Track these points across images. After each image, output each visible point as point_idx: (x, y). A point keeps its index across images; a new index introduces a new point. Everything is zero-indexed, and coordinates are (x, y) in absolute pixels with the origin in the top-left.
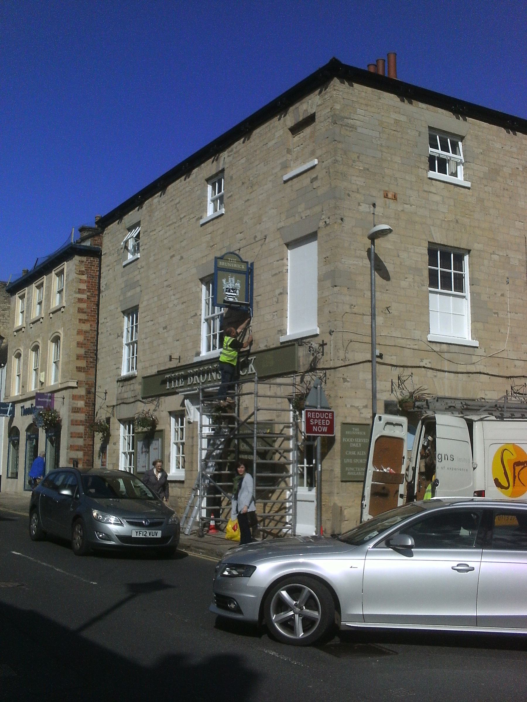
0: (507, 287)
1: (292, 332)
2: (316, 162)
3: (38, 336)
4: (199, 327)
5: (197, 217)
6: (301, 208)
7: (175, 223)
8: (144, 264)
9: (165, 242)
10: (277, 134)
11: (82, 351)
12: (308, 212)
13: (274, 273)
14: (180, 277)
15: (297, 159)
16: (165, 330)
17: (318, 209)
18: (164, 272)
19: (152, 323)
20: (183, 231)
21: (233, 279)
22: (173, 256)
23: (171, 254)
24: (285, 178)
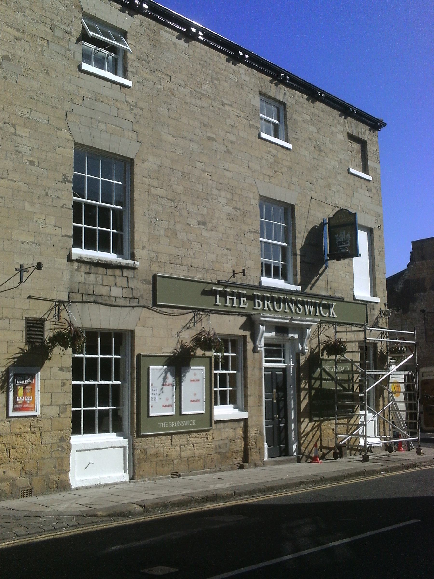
14: (226, 173)
16: (203, 227)
24: (352, 171)
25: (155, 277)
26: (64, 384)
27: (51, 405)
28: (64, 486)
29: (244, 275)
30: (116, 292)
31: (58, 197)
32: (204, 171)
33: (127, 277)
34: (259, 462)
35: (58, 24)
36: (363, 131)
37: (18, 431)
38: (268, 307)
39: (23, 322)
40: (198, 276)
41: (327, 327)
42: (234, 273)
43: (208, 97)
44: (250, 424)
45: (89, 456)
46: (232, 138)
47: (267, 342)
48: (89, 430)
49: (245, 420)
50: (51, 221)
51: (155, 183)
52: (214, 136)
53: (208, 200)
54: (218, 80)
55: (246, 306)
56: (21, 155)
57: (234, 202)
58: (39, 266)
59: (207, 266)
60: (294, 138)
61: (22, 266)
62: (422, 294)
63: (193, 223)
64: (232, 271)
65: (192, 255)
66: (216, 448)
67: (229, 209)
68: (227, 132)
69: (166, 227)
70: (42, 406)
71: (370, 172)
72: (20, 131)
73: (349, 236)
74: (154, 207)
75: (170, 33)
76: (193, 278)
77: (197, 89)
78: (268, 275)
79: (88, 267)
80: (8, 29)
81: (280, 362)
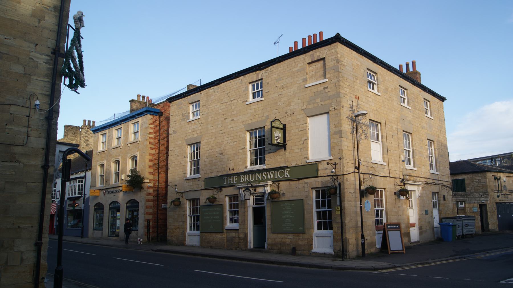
0: (392, 139)
1: (312, 157)
2: (327, 80)
3: (119, 156)
4: (246, 154)
6: (318, 101)
8: (203, 121)
9: (220, 111)
10: (299, 65)
11: (151, 164)
12: (323, 103)
13: (300, 130)
14: (231, 129)
15: (312, 77)
17: (330, 101)
18: (219, 126)
20: (233, 107)
22: (226, 118)
44: (240, 232)
46: (233, 113)
51: (206, 147)
81: (263, 204)
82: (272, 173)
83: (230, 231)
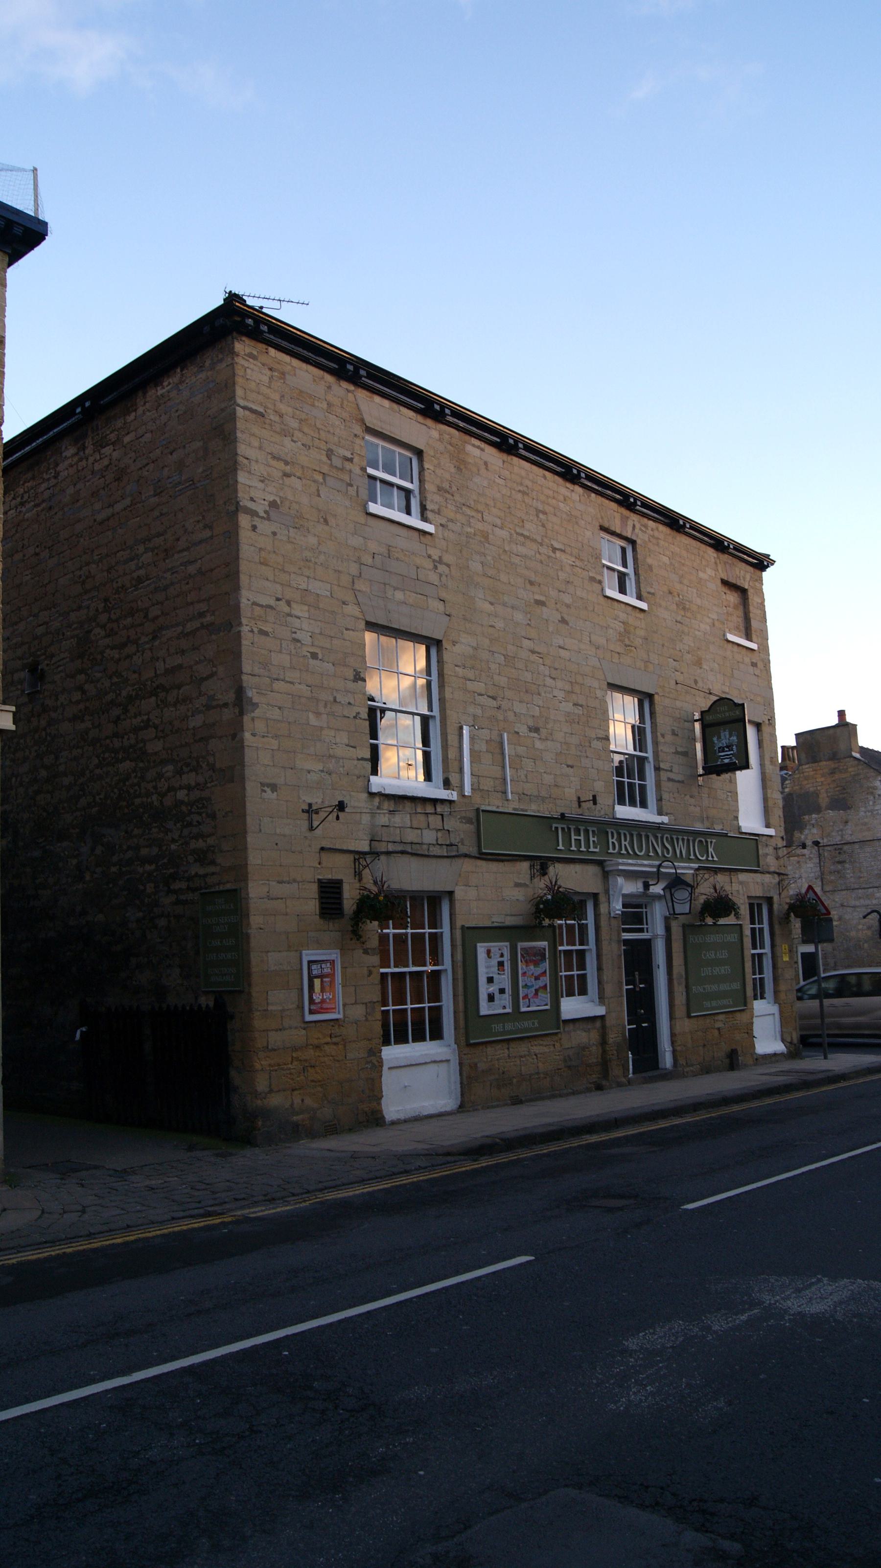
5: (591, 575)
7: (541, 544)
14: (563, 653)
16: (536, 735)
19: (494, 703)
21: (727, 733)
23: (537, 597)
25: (478, 810)
26: (370, 973)
27: (356, 1003)
28: (376, 1119)
29: (595, 803)
30: (429, 837)
31: (349, 703)
32: (533, 652)
33: (442, 815)
34: (624, 1080)
35: (334, 448)
36: (741, 574)
37: (316, 1042)
38: (626, 849)
39: (316, 885)
40: (533, 809)
41: (706, 876)
42: (579, 802)
43: (535, 541)
44: (609, 1022)
45: (405, 1077)
46: (567, 599)
47: (628, 900)
48: (401, 1039)
49: (602, 1017)
50: (343, 738)
52: (542, 598)
53: (539, 694)
54: (545, 513)
55: (597, 850)
56: (299, 645)
57: (574, 696)
58: (341, 806)
59: (544, 793)
60: (649, 593)
61: (310, 805)
62: (814, 816)
63: (523, 730)
64: (575, 799)
65: (523, 777)
66: (565, 1061)
67: (568, 707)
68: (560, 591)
69: (488, 738)
70: (344, 1005)
71: (754, 637)
72: (299, 610)
73: (734, 738)
74: (471, 710)
75: (478, 447)
76: (526, 811)
77: (518, 530)
78: (621, 802)
79: (392, 803)
80: (274, 463)
81: (641, 930)
82: (683, 839)
83: (571, 1027)
